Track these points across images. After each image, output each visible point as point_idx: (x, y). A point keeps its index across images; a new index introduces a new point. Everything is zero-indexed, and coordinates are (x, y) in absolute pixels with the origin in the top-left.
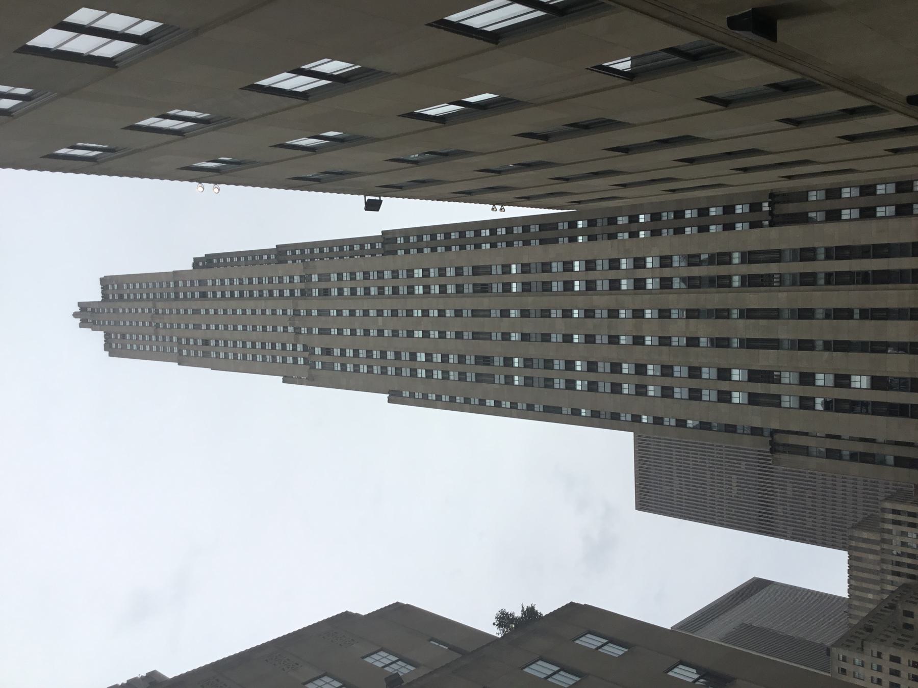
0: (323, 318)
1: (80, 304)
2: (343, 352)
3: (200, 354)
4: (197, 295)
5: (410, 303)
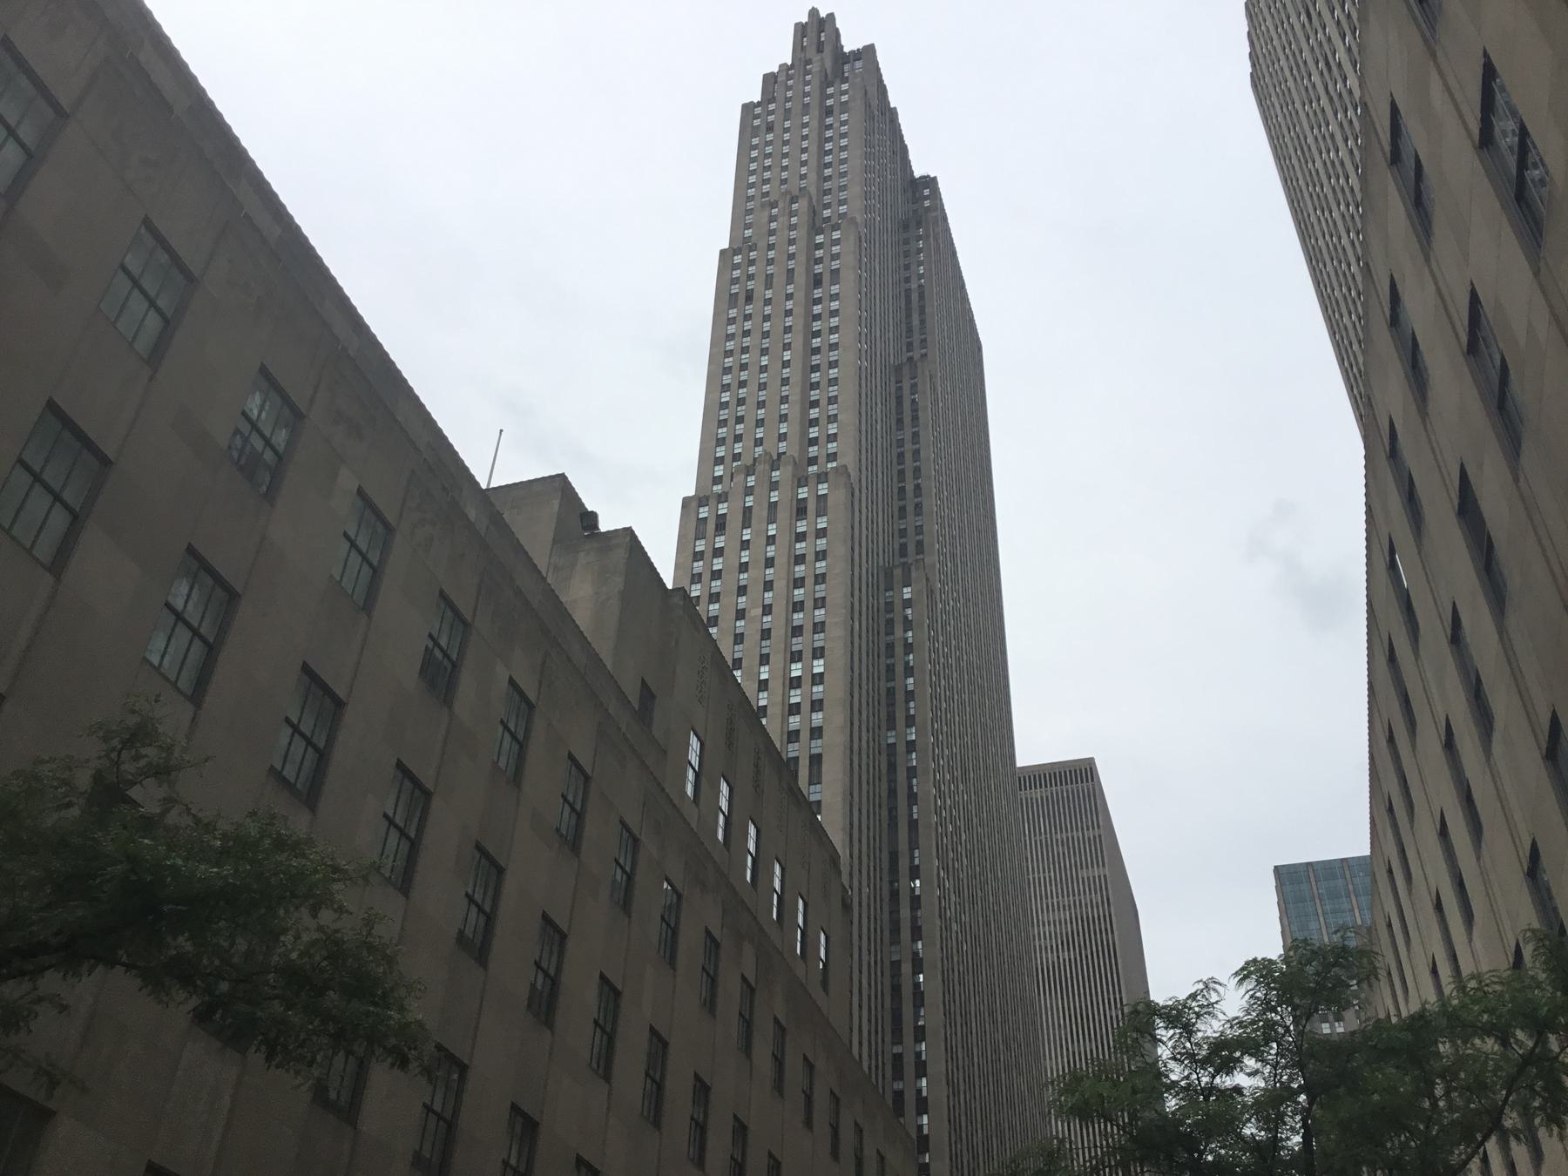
0: (765, 513)
1: (831, 16)
2: (718, 552)
3: (735, 289)
4: (818, 269)
5: (777, 659)
